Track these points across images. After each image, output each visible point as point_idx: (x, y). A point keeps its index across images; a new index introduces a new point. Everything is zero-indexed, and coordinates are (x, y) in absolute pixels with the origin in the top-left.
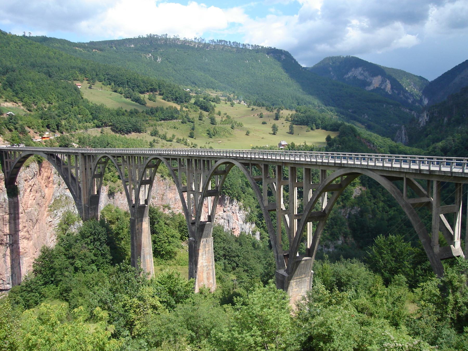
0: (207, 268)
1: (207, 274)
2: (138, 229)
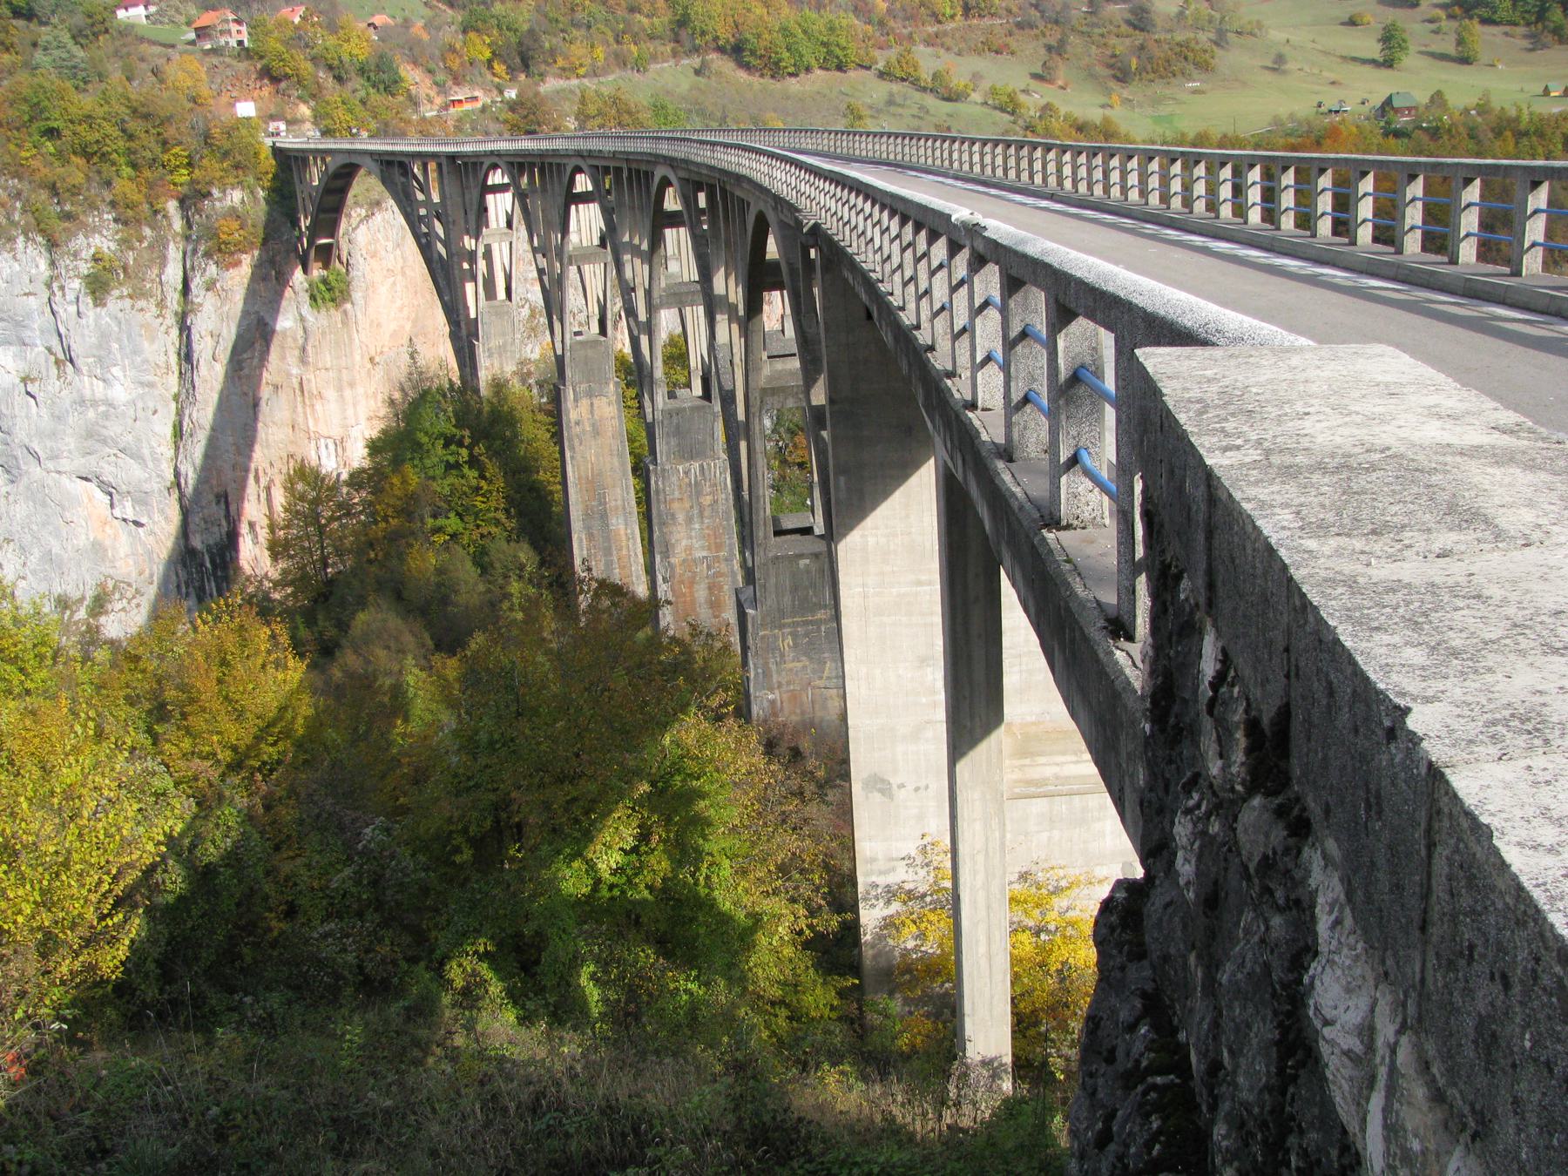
0: (709, 568)
1: (710, 588)
2: (577, 423)
